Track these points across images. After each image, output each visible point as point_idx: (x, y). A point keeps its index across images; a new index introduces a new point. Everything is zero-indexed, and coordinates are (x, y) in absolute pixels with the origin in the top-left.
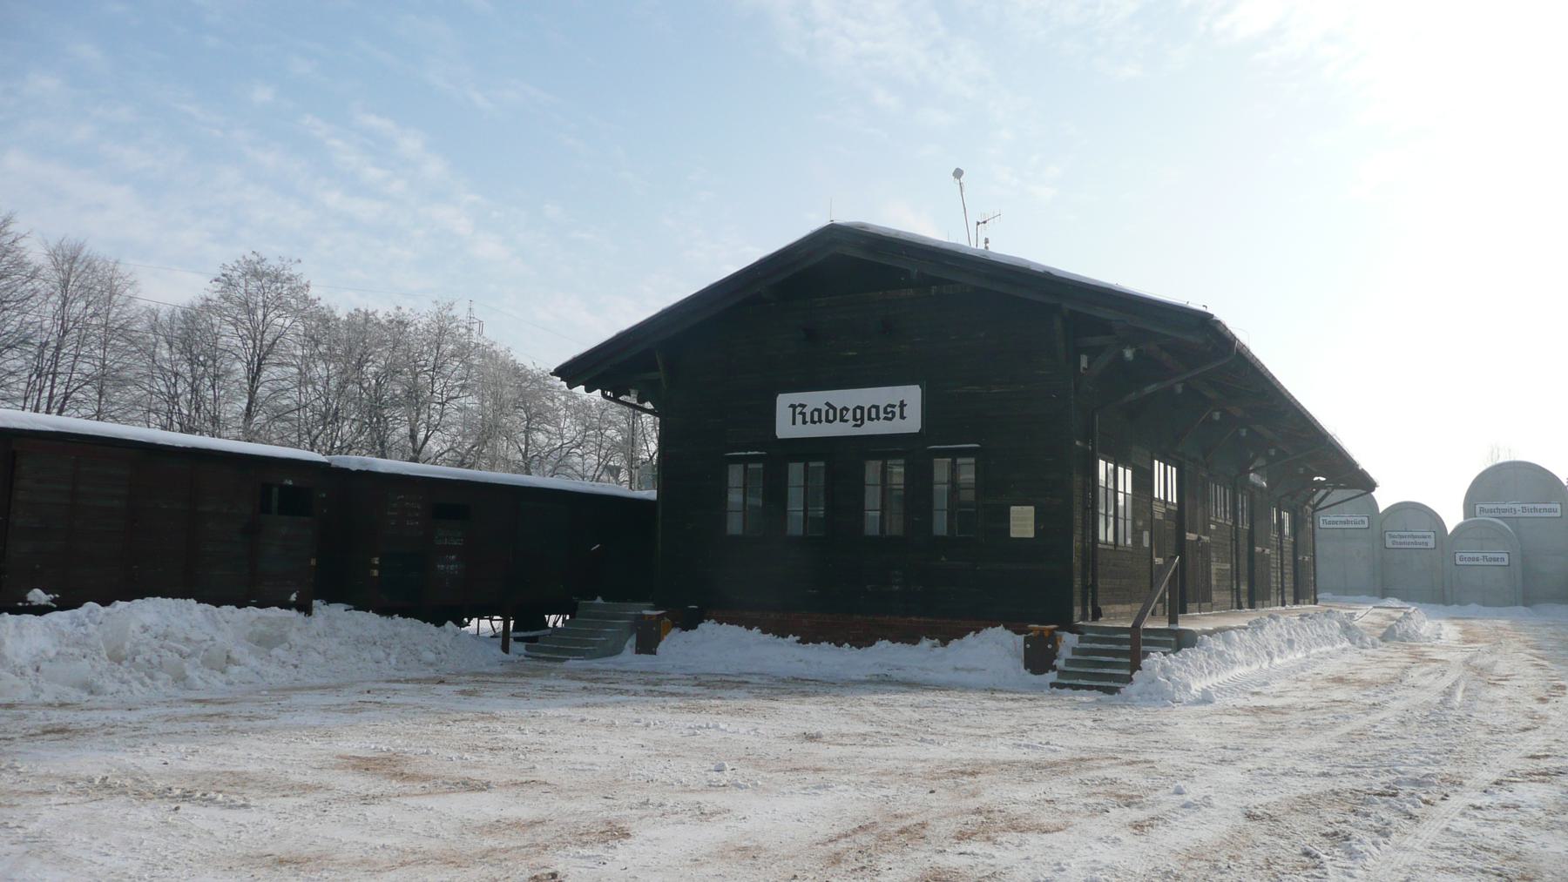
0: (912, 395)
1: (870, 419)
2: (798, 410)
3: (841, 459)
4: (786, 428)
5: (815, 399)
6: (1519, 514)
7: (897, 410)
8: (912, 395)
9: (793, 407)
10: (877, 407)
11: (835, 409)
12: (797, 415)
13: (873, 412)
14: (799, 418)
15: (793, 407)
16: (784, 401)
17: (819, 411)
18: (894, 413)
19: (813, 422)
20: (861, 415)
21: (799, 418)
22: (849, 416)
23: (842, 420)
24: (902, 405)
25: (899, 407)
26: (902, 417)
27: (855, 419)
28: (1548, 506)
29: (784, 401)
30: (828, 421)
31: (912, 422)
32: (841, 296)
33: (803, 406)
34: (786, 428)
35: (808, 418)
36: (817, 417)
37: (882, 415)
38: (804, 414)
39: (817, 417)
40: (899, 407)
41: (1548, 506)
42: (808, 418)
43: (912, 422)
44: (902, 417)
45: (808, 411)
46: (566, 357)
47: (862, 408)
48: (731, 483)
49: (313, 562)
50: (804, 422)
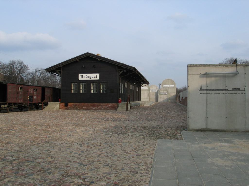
0: (98, 75)
2: (82, 76)
3: (88, 83)
4: (80, 78)
5: (84, 75)
6: (169, 87)
7: (96, 77)
8: (98, 75)
9: (81, 76)
10: (93, 76)
11: (87, 76)
12: (82, 77)
13: (92, 77)
14: (82, 77)
15: (81, 76)
16: (80, 75)
17: (85, 76)
19: (84, 78)
20: (91, 77)
22: (89, 77)
23: (88, 78)
24: (96, 76)
25: (96, 76)
26: (96, 77)
28: (173, 85)
29: (80, 75)
30: (86, 78)
31: (98, 78)
32: (88, 61)
33: (83, 76)
34: (80, 78)
35: (83, 77)
36: (85, 77)
38: (83, 77)
40: (96, 76)
41: (173, 85)
42: (83, 77)
43: (98, 78)
44: (96, 77)
45: (83, 76)
49: (23, 97)
50: (83, 78)
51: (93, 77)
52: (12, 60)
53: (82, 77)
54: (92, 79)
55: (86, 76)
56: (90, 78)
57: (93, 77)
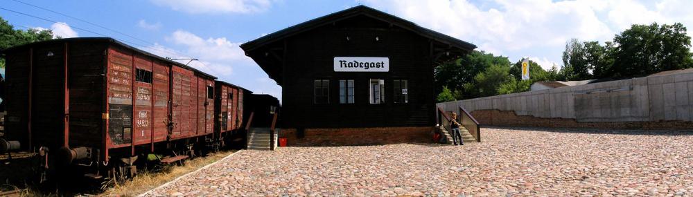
0: (386, 61)
3: (362, 80)
4: (337, 68)
5: (349, 60)
7: (381, 65)
8: (386, 61)
9: (341, 62)
11: (358, 64)
13: (372, 65)
14: (343, 65)
15: (341, 62)
16: (337, 60)
17: (352, 63)
19: (349, 66)
21: (343, 65)
22: (363, 65)
24: (383, 63)
26: (383, 67)
29: (337, 60)
31: (386, 69)
34: (337, 68)
36: (350, 65)
38: (345, 64)
39: (350, 65)
40: (383, 64)
43: (386, 69)
44: (383, 67)
46: (246, 41)
48: (341, 94)
54: (371, 70)
55: (354, 63)
56: (364, 68)
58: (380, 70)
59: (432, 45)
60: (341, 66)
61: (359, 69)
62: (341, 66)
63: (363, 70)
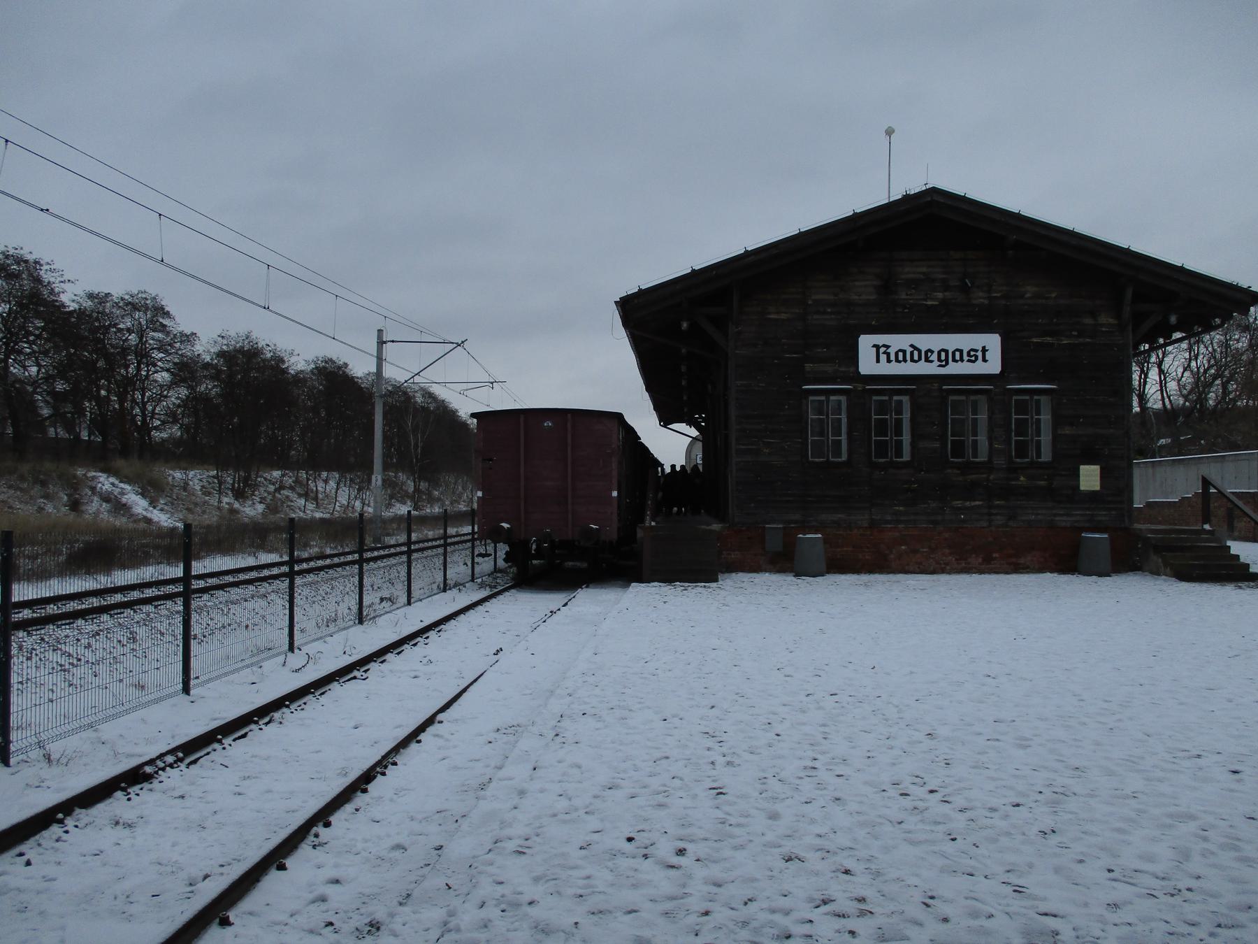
0: (993, 342)
1: (954, 360)
2: (882, 350)
3: (932, 394)
4: (868, 364)
5: (899, 341)
7: (980, 354)
8: (993, 342)
9: (877, 347)
10: (961, 351)
11: (920, 351)
12: (875, 355)
13: (958, 355)
14: (883, 357)
15: (877, 347)
16: (866, 343)
17: (904, 352)
18: (977, 357)
19: (897, 360)
20: (945, 357)
21: (883, 357)
22: (934, 357)
23: (927, 360)
24: (984, 350)
25: (982, 352)
26: (984, 360)
27: (939, 359)
30: (912, 360)
31: (993, 366)
33: (888, 347)
34: (868, 364)
35: (893, 357)
37: (966, 358)
38: (888, 355)
40: (982, 352)
42: (893, 357)
43: (993, 366)
44: (984, 360)
45: (892, 351)
47: (946, 352)
50: (889, 361)
51: (958, 357)
52: (153, 291)
53: (875, 355)
54: (954, 369)
55: (909, 350)
57: (958, 354)
58: (978, 368)
59: (1129, 294)
60: (878, 361)
61: (922, 368)
62: (878, 361)
63: (932, 369)
